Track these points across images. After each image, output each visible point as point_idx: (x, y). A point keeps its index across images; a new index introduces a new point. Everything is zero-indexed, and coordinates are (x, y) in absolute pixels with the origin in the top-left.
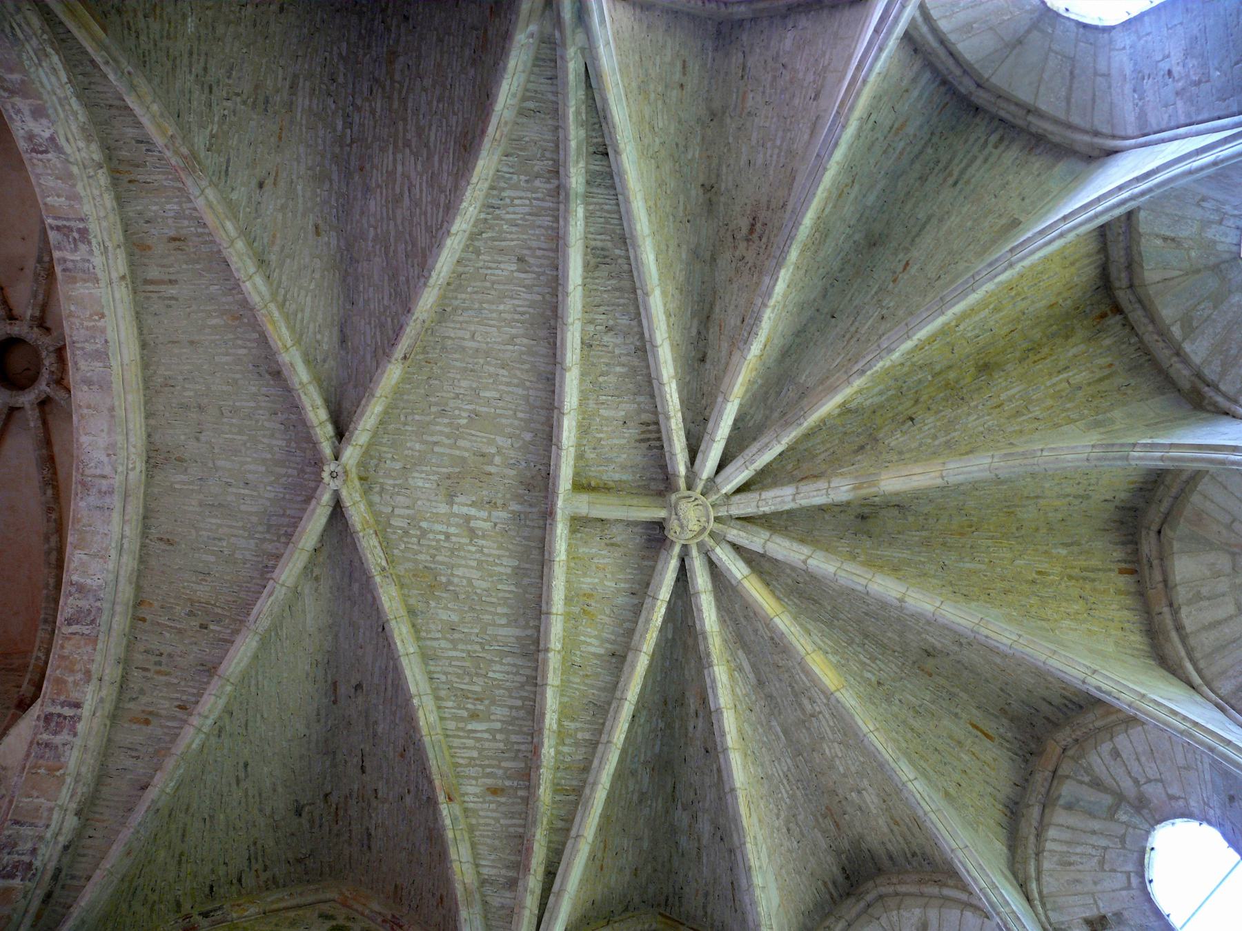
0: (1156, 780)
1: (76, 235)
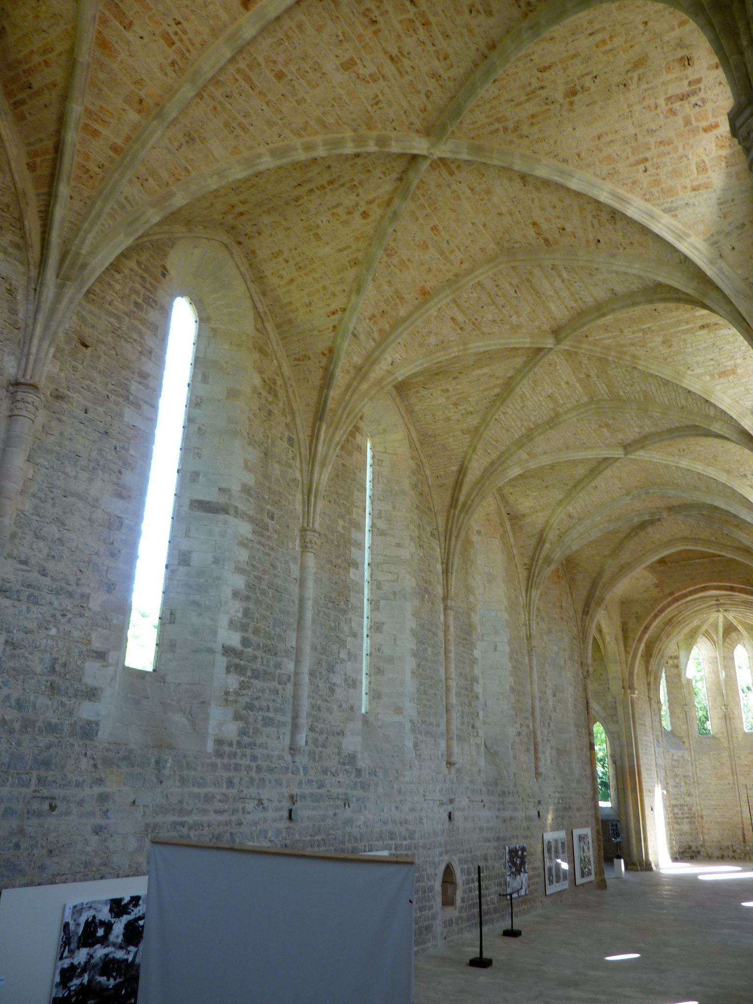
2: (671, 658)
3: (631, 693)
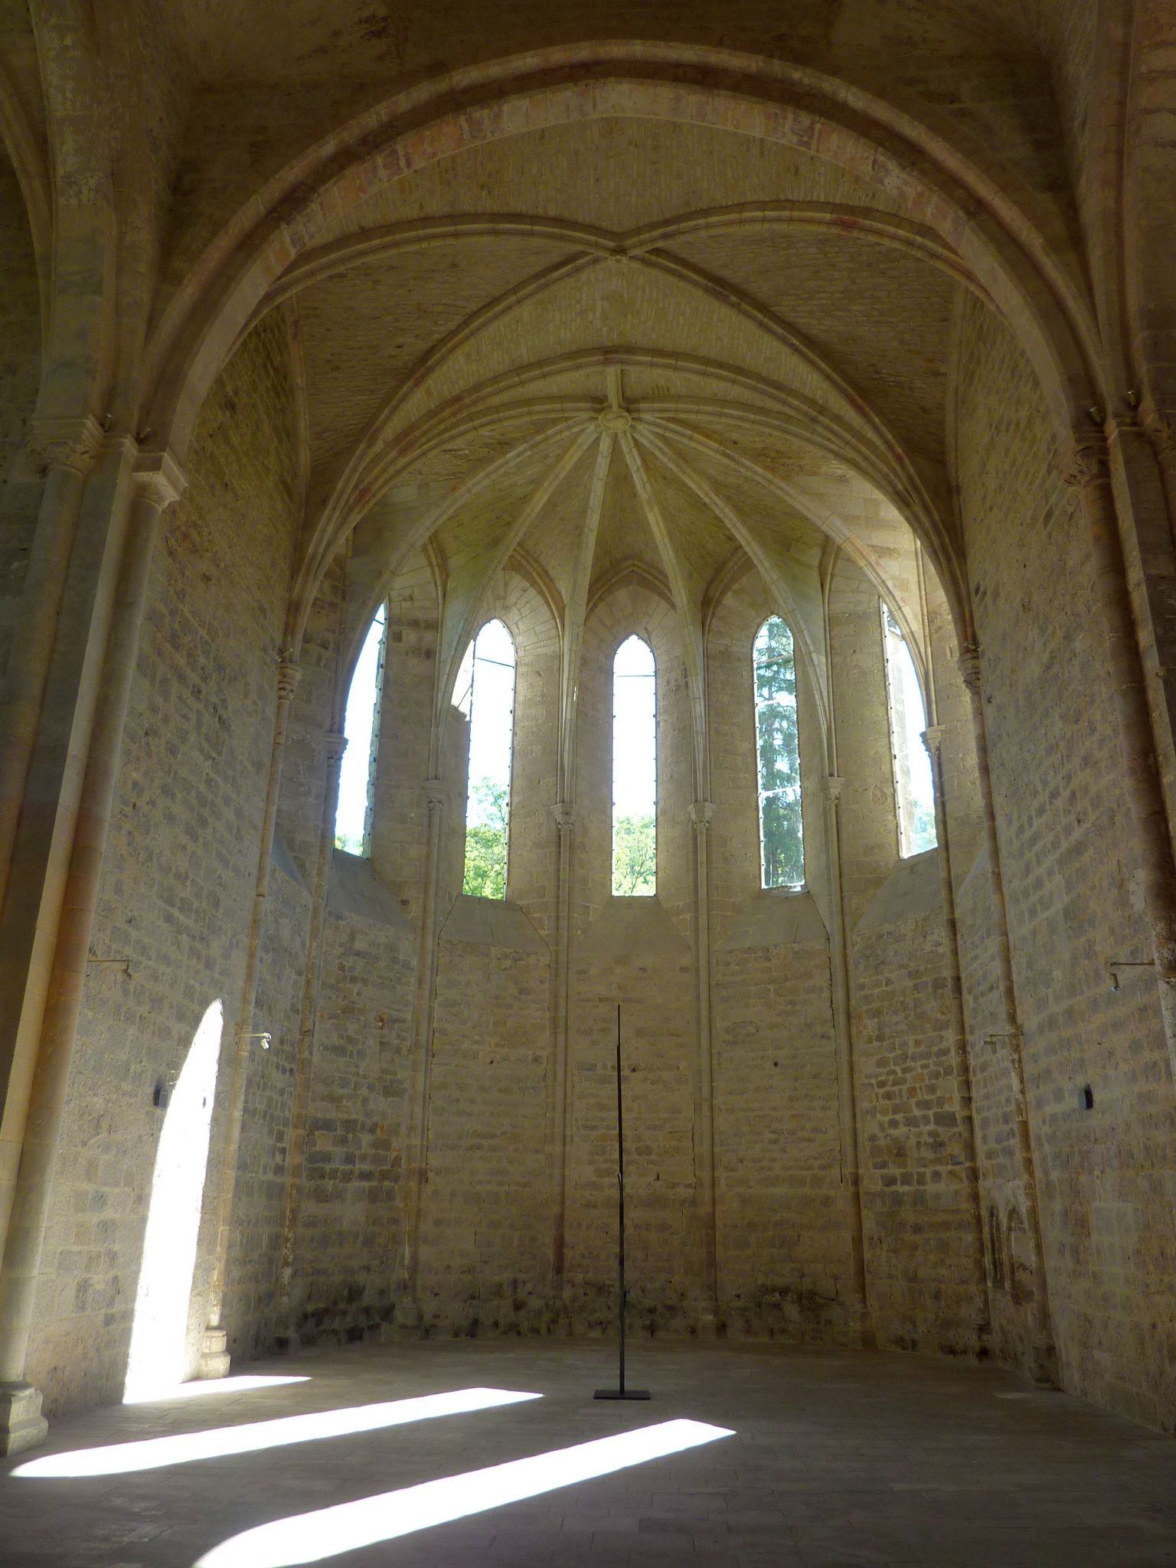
1: (805, 139)
2: (415, 624)
3: (138, 467)
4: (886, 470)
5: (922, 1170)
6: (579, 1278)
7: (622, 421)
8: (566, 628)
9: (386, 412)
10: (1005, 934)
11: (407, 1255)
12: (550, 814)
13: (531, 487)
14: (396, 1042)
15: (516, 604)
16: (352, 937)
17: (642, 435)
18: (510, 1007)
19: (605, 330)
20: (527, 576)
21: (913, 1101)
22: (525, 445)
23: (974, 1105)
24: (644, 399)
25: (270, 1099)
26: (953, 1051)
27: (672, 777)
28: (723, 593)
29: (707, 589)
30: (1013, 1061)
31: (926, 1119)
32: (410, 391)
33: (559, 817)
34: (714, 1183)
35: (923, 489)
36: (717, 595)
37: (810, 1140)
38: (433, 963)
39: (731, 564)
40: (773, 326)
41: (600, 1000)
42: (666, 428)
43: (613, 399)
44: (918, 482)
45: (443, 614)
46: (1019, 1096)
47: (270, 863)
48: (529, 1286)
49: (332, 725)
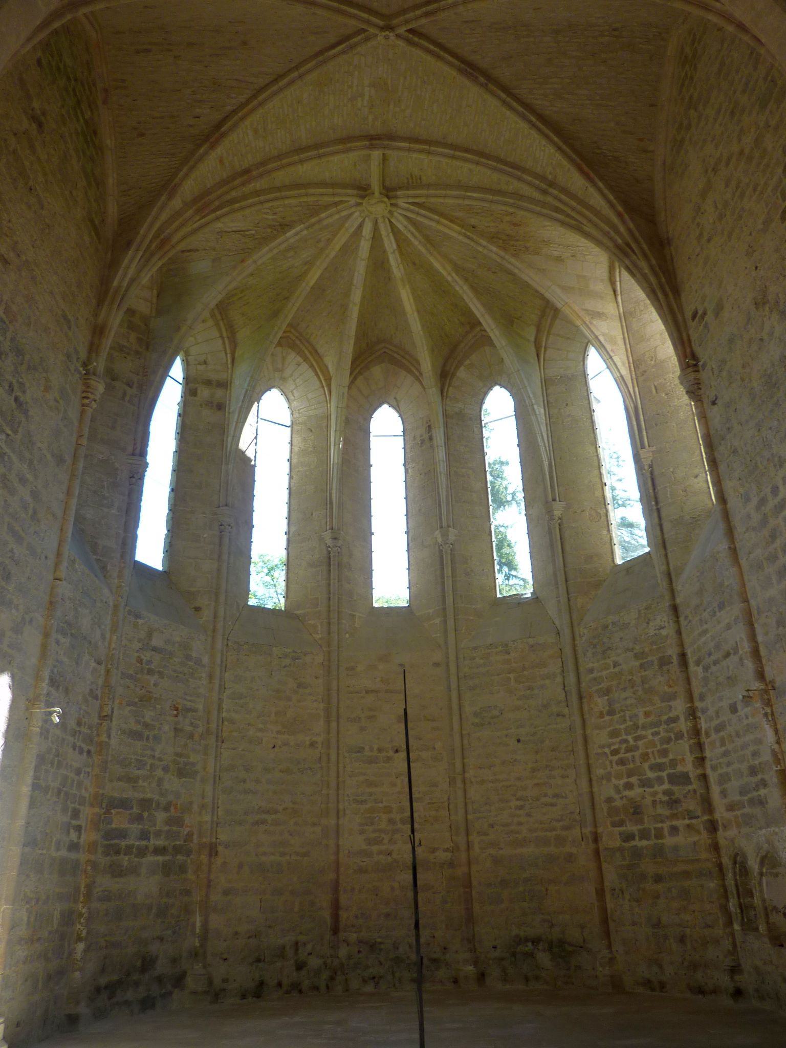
0: (296, 385)
2: (209, 383)
4: (607, 229)
5: (660, 825)
6: (353, 937)
7: (383, 205)
8: (333, 393)
9: (185, 170)
10: (746, 601)
11: (198, 924)
12: (321, 539)
13: (306, 267)
14: (189, 728)
15: (291, 375)
16: (150, 635)
17: (398, 220)
18: (289, 699)
19: (371, 118)
20: (300, 353)
21: (646, 766)
22: (302, 225)
23: (708, 764)
24: (400, 188)
25: (65, 778)
26: (682, 719)
27: (420, 511)
28: (457, 367)
29: (444, 365)
30: (766, 715)
31: (660, 780)
32: (206, 153)
33: (329, 542)
34: (469, 846)
35: (640, 239)
36: (453, 369)
37: (552, 805)
38: (222, 662)
39: (462, 345)
40: (515, 104)
41: (367, 692)
42: (418, 214)
43: (376, 186)
44: (637, 234)
45: (232, 375)
46: (776, 747)
47: (68, 550)
48: (309, 947)
49: (135, 449)
